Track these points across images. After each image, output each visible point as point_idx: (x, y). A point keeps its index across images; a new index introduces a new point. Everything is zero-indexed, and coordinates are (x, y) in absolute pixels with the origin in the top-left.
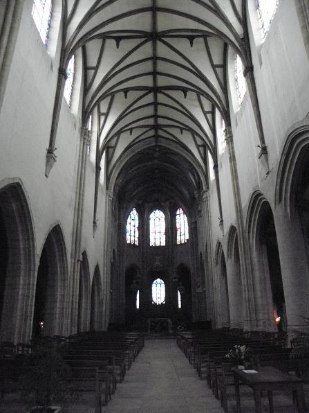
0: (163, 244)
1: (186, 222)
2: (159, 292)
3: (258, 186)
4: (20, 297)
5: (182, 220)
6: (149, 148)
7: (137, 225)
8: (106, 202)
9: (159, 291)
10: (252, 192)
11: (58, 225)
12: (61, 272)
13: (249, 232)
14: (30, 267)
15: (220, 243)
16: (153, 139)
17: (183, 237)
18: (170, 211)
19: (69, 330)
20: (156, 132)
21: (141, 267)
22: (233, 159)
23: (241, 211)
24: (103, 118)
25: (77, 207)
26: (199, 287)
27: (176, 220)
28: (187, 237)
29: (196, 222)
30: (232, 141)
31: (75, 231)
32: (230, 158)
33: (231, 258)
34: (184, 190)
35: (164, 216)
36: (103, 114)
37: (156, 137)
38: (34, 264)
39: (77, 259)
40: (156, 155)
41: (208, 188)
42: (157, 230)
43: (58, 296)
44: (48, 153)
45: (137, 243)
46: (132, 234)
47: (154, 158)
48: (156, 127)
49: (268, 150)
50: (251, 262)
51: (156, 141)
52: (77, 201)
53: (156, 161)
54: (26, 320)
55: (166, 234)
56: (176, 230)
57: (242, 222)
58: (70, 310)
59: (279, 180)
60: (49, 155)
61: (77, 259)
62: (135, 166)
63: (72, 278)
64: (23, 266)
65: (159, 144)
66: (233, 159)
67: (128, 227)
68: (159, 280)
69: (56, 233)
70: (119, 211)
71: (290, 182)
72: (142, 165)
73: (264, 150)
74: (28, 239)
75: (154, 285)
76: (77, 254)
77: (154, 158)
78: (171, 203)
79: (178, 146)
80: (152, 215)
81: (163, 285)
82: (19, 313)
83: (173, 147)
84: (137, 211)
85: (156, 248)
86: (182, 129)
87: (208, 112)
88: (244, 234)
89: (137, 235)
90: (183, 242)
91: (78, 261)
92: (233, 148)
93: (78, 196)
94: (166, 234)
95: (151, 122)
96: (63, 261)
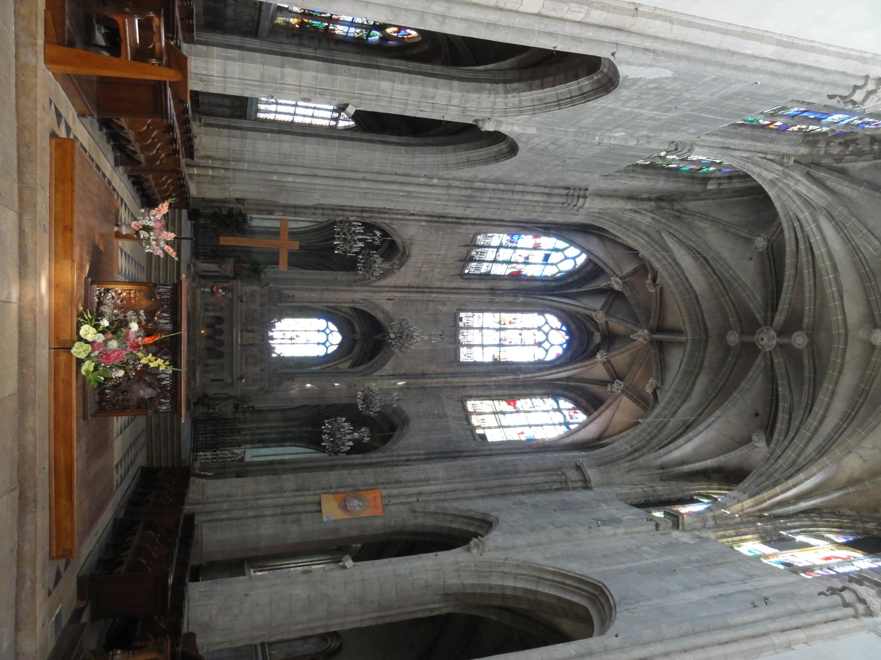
0: (465, 355)
2: (303, 338)
5: (544, 420)
7: (529, 271)
8: (862, 59)
9: (303, 337)
17: (490, 420)
18: (568, 379)
26: (344, 507)
27: (542, 396)
28: (493, 436)
29: (586, 485)
34: (696, 442)
35: (551, 356)
42: (511, 336)
45: (472, 268)
46: (504, 254)
55: (499, 367)
56: (511, 399)
67: (527, 240)
68: (336, 338)
70: (631, 197)
72: (849, 281)
75: (321, 323)
78: (603, 383)
81: (321, 351)
84: (570, 274)
85: (454, 328)
89: (499, 270)
90: (475, 420)
94: (496, 362)
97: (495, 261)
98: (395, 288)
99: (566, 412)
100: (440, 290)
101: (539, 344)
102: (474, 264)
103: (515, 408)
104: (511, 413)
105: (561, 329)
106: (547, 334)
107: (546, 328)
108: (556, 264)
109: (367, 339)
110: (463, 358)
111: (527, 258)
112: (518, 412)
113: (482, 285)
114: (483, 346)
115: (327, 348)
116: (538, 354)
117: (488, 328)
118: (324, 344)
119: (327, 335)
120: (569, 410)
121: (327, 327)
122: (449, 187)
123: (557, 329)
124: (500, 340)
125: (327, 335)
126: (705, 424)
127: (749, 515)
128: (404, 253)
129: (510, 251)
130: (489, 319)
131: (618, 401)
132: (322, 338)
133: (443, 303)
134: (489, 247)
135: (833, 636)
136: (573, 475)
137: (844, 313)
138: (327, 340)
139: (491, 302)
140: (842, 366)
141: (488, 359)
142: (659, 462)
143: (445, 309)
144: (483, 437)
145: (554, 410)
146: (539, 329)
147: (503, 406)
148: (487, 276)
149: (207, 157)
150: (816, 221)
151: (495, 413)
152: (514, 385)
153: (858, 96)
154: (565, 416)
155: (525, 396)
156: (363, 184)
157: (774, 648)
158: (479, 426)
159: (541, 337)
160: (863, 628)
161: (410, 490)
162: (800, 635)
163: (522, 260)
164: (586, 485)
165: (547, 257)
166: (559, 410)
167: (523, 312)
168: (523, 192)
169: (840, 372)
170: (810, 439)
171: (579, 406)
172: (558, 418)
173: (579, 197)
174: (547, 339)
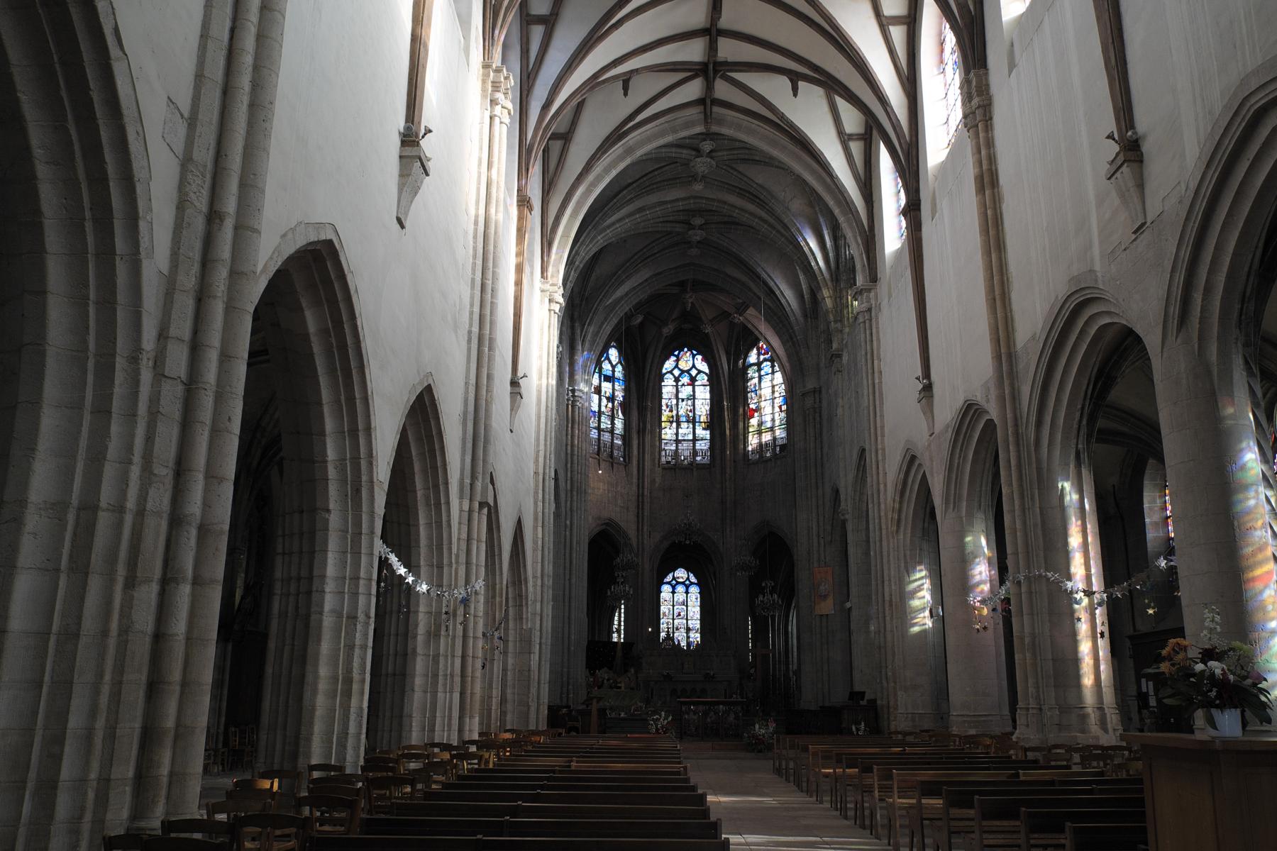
1: (781, 390)
3: (1092, 271)
4: (328, 621)
6: (678, 145)
7: (620, 395)
10: (1062, 291)
11: (429, 389)
12: (430, 538)
13: (1039, 423)
14: (358, 524)
15: (913, 458)
16: (694, 112)
18: (728, 354)
19: (455, 722)
20: (709, 87)
21: (632, 533)
22: (988, 181)
23: (1011, 356)
24: (537, 32)
25: (475, 329)
26: (825, 597)
29: (817, 391)
30: (988, 120)
31: (471, 408)
32: (980, 180)
33: (956, 506)
35: (704, 367)
36: (540, 20)
37: (706, 102)
38: (372, 513)
39: (478, 498)
40: (702, 165)
41: (874, 278)
42: (684, 408)
43: (421, 616)
44: (404, 143)
47: (694, 178)
48: (710, 70)
49: (1146, 147)
50: (1043, 522)
51: (707, 117)
52: (476, 309)
53: (698, 187)
54: (348, 694)
55: (714, 423)
57: (1015, 397)
58: (458, 662)
59: (1186, 253)
60: (409, 151)
61: (478, 498)
62: (630, 201)
63: (463, 559)
64: (334, 520)
65: (715, 129)
66: (988, 181)
68: (681, 574)
69: (424, 410)
71: (1227, 260)
73: (1131, 150)
74: (354, 432)
75: (666, 589)
76: (479, 485)
77: (694, 178)
79: (784, 140)
80: (669, 364)
81: (695, 590)
82: (324, 671)
83: (759, 139)
86: (795, 78)
87: (896, 20)
88: (1022, 430)
89: (619, 424)
91: (482, 505)
92: (990, 143)
93: (478, 293)
94: (710, 426)
95: (694, 51)
96: (438, 505)
97: (612, 431)
98: (639, 530)
99: (762, 357)
100: (640, 485)
101: (693, 380)
102: (616, 453)
103: (756, 411)
104: (761, 416)
105: (677, 356)
106: (683, 372)
107: (676, 372)
108: (613, 367)
109: (686, 552)
110: (707, 460)
111: (608, 399)
112: (758, 409)
113: (635, 443)
114: (695, 440)
115: (692, 583)
116: (702, 379)
117: (677, 434)
118: (687, 587)
119: (678, 583)
120: (759, 354)
121: (669, 583)
122: (571, 510)
123: (677, 361)
124: (688, 421)
125: (678, 583)
126: (769, 280)
127: (835, 290)
128: (607, 524)
129: (603, 419)
130: (668, 433)
131: (750, 318)
132: (680, 589)
133: (653, 481)
134: (599, 439)
135: (878, 340)
136: (809, 402)
137: (677, 200)
138: (683, 583)
139: (652, 432)
140: (719, 201)
141: (707, 434)
142: (801, 319)
143: (658, 480)
144: (783, 447)
145: (759, 370)
146: (677, 380)
147: (754, 422)
148: (626, 437)
149: (561, 698)
150: (605, 230)
151: (760, 433)
152: (734, 410)
153: (557, 308)
154: (765, 360)
155: (746, 399)
156: (573, 581)
157: (881, 382)
158: (774, 450)
159: (685, 380)
160: (877, 318)
161: (815, 544)
162: (876, 362)
163: (610, 405)
164: (817, 391)
165: (608, 379)
166: (759, 364)
167: (661, 398)
168: (572, 446)
169: (725, 203)
170: (778, 231)
171: (754, 343)
172: (767, 367)
173: (574, 396)
174: (688, 371)
